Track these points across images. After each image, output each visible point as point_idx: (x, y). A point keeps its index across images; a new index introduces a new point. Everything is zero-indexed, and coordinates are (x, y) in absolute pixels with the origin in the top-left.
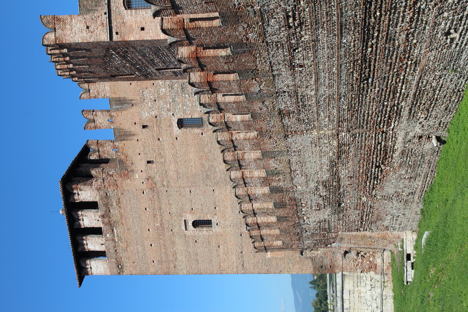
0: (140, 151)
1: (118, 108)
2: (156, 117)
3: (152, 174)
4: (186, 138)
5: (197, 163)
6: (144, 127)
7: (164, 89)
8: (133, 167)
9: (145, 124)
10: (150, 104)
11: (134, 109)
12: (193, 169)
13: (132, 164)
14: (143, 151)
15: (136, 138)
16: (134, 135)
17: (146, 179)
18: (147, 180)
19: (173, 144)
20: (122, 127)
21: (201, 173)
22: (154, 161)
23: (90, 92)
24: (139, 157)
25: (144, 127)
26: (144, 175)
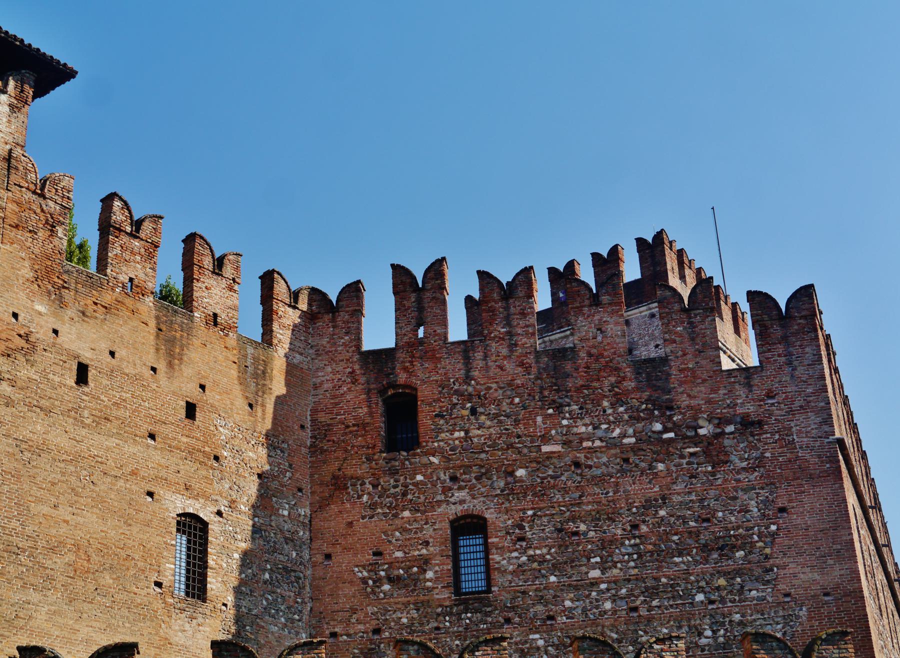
0: (122, 359)
1: (245, 356)
2: (216, 458)
3: (44, 359)
4: (148, 526)
5: (64, 530)
6: (191, 410)
7: (286, 513)
8: (70, 312)
9: (198, 414)
10: (251, 454)
11: (241, 403)
12: (46, 510)
13: (83, 313)
14: (120, 370)
15: (162, 366)
16: (170, 365)
17: (26, 330)
18: (22, 332)
19: (134, 473)
20: (196, 342)
21: (29, 530)
22: (86, 389)
23: (290, 306)
24: (105, 346)
25: (191, 410)
26: (42, 334)
